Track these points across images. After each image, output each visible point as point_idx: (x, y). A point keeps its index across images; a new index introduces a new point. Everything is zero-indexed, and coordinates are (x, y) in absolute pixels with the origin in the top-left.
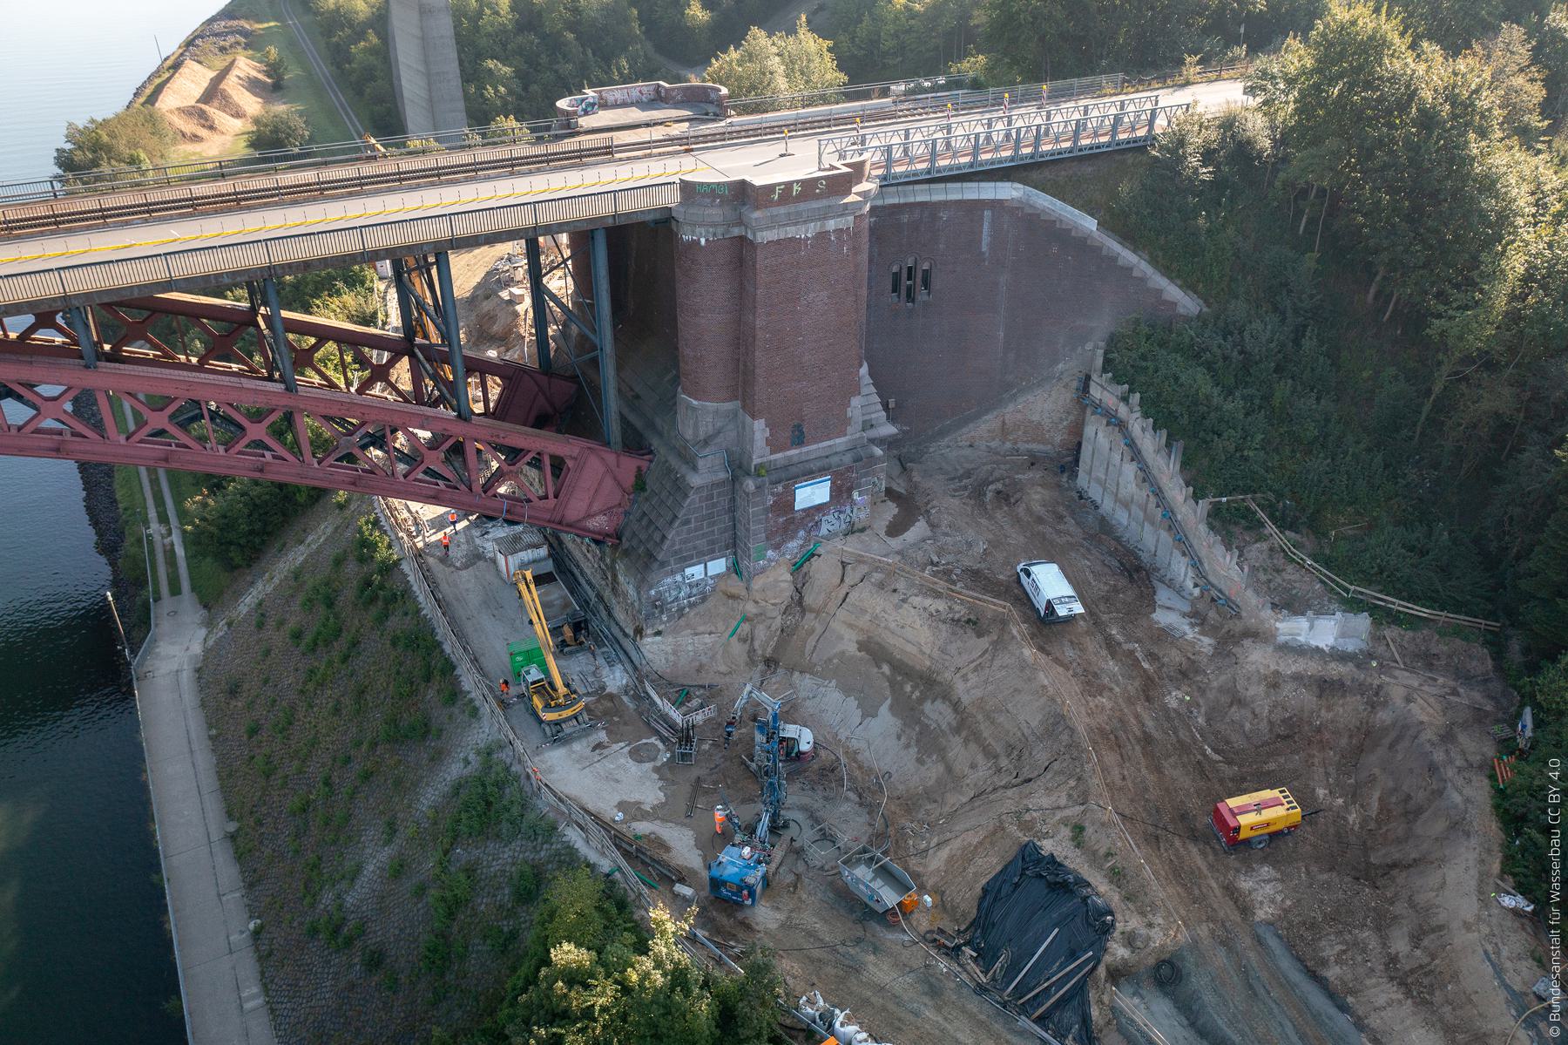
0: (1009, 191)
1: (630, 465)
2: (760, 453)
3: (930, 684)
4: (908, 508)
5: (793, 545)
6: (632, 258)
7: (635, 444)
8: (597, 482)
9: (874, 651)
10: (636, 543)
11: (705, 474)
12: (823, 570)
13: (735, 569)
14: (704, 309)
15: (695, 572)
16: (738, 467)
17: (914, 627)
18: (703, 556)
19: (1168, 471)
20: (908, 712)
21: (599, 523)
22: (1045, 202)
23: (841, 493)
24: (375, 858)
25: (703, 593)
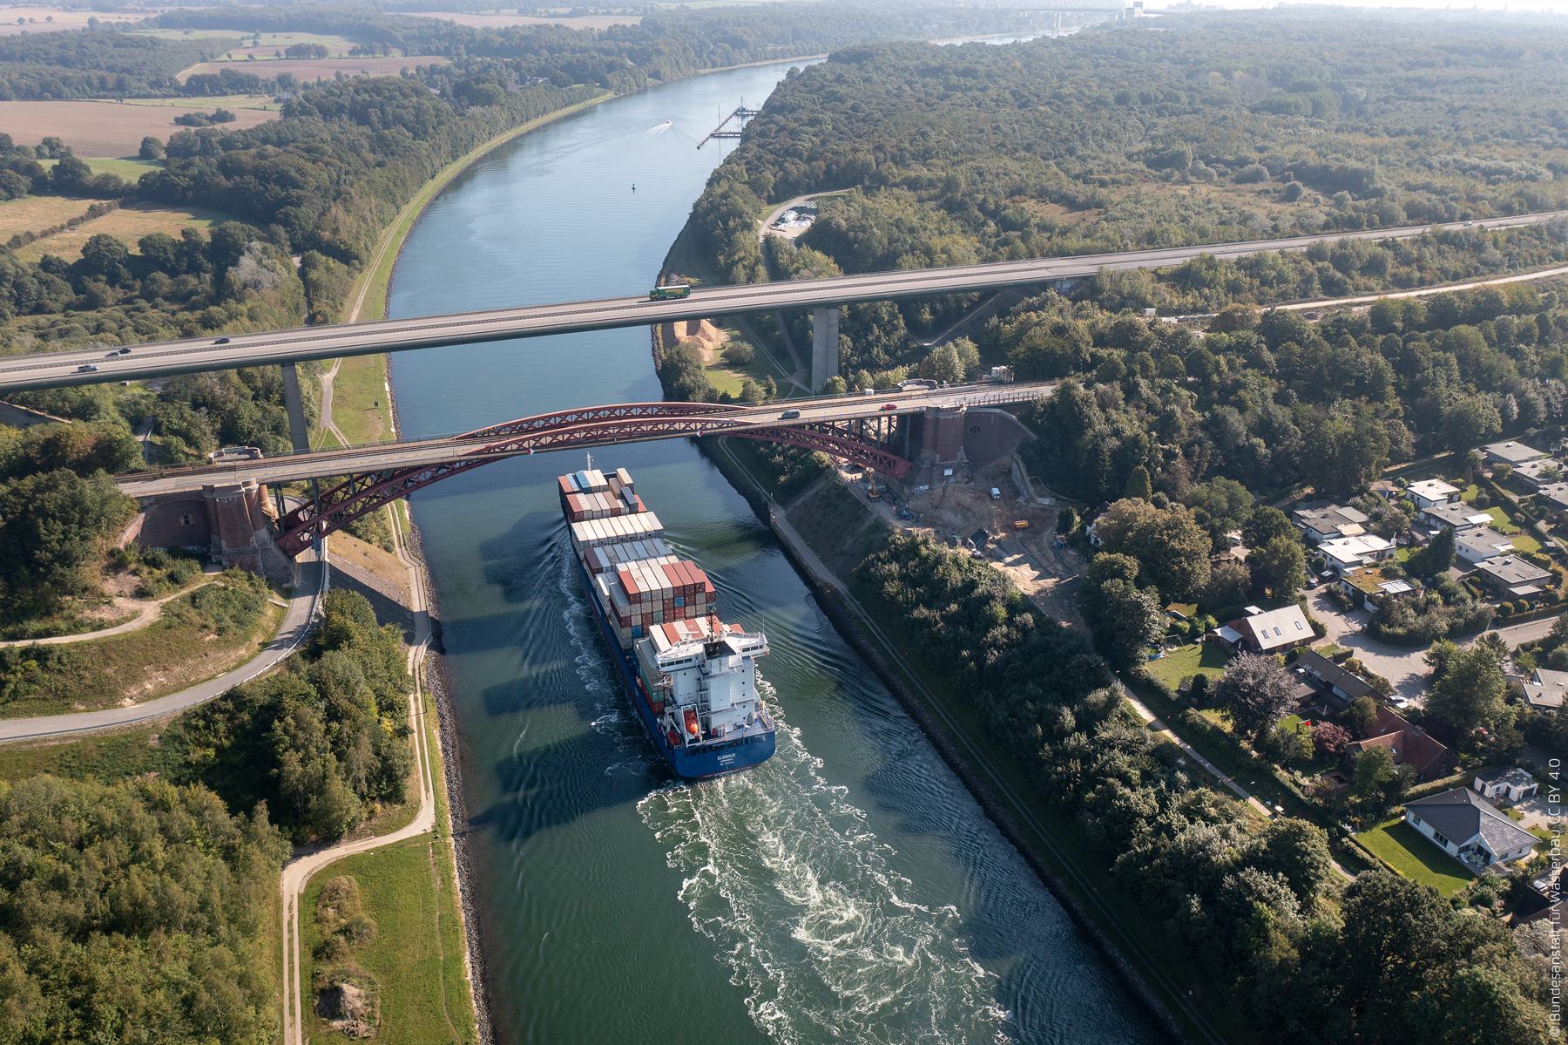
0: (998, 411)
3: (968, 509)
4: (971, 479)
6: (913, 423)
7: (910, 460)
8: (902, 466)
9: (958, 504)
10: (909, 481)
11: (926, 465)
12: (950, 489)
14: (929, 431)
16: (933, 465)
17: (967, 499)
19: (1024, 470)
20: (964, 515)
24: (849, 541)
25: (923, 493)
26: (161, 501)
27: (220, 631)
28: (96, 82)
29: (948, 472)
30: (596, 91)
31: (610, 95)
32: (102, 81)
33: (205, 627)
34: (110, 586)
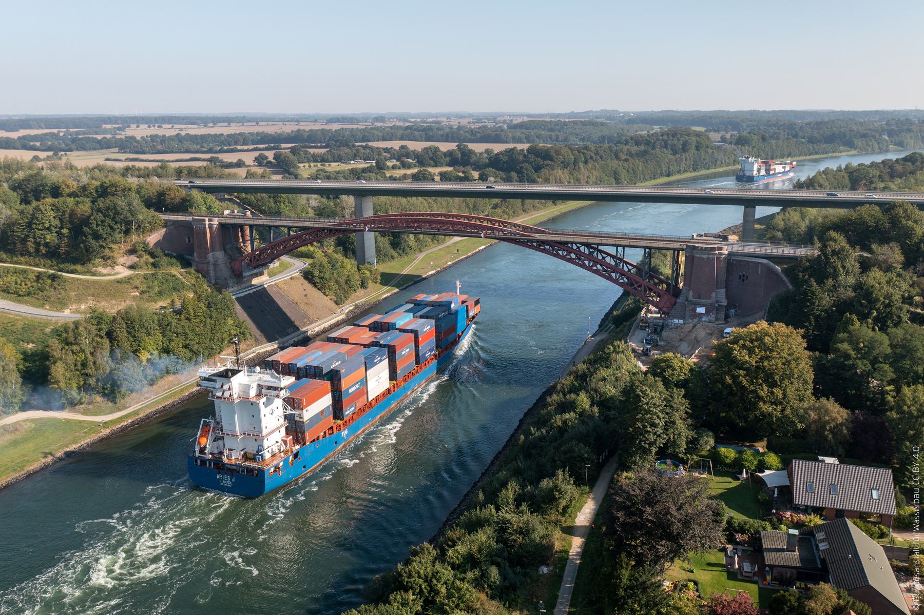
0: (765, 261)
1: (673, 299)
2: (690, 298)
5: (696, 320)
9: (695, 338)
13: (684, 324)
15: (676, 321)
18: (679, 318)
21: (665, 309)
22: (771, 264)
23: (708, 312)
25: (677, 327)
26: (175, 222)
27: (142, 293)
28: (554, 137)
29: (701, 310)
30: (842, 148)
31: (854, 152)
32: (557, 137)
33: (137, 288)
34: (122, 260)
